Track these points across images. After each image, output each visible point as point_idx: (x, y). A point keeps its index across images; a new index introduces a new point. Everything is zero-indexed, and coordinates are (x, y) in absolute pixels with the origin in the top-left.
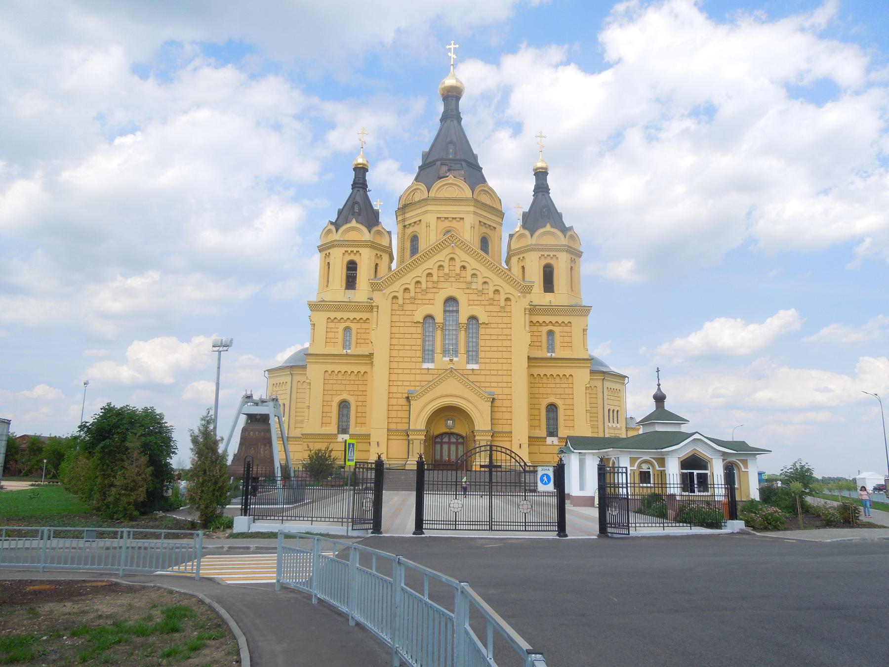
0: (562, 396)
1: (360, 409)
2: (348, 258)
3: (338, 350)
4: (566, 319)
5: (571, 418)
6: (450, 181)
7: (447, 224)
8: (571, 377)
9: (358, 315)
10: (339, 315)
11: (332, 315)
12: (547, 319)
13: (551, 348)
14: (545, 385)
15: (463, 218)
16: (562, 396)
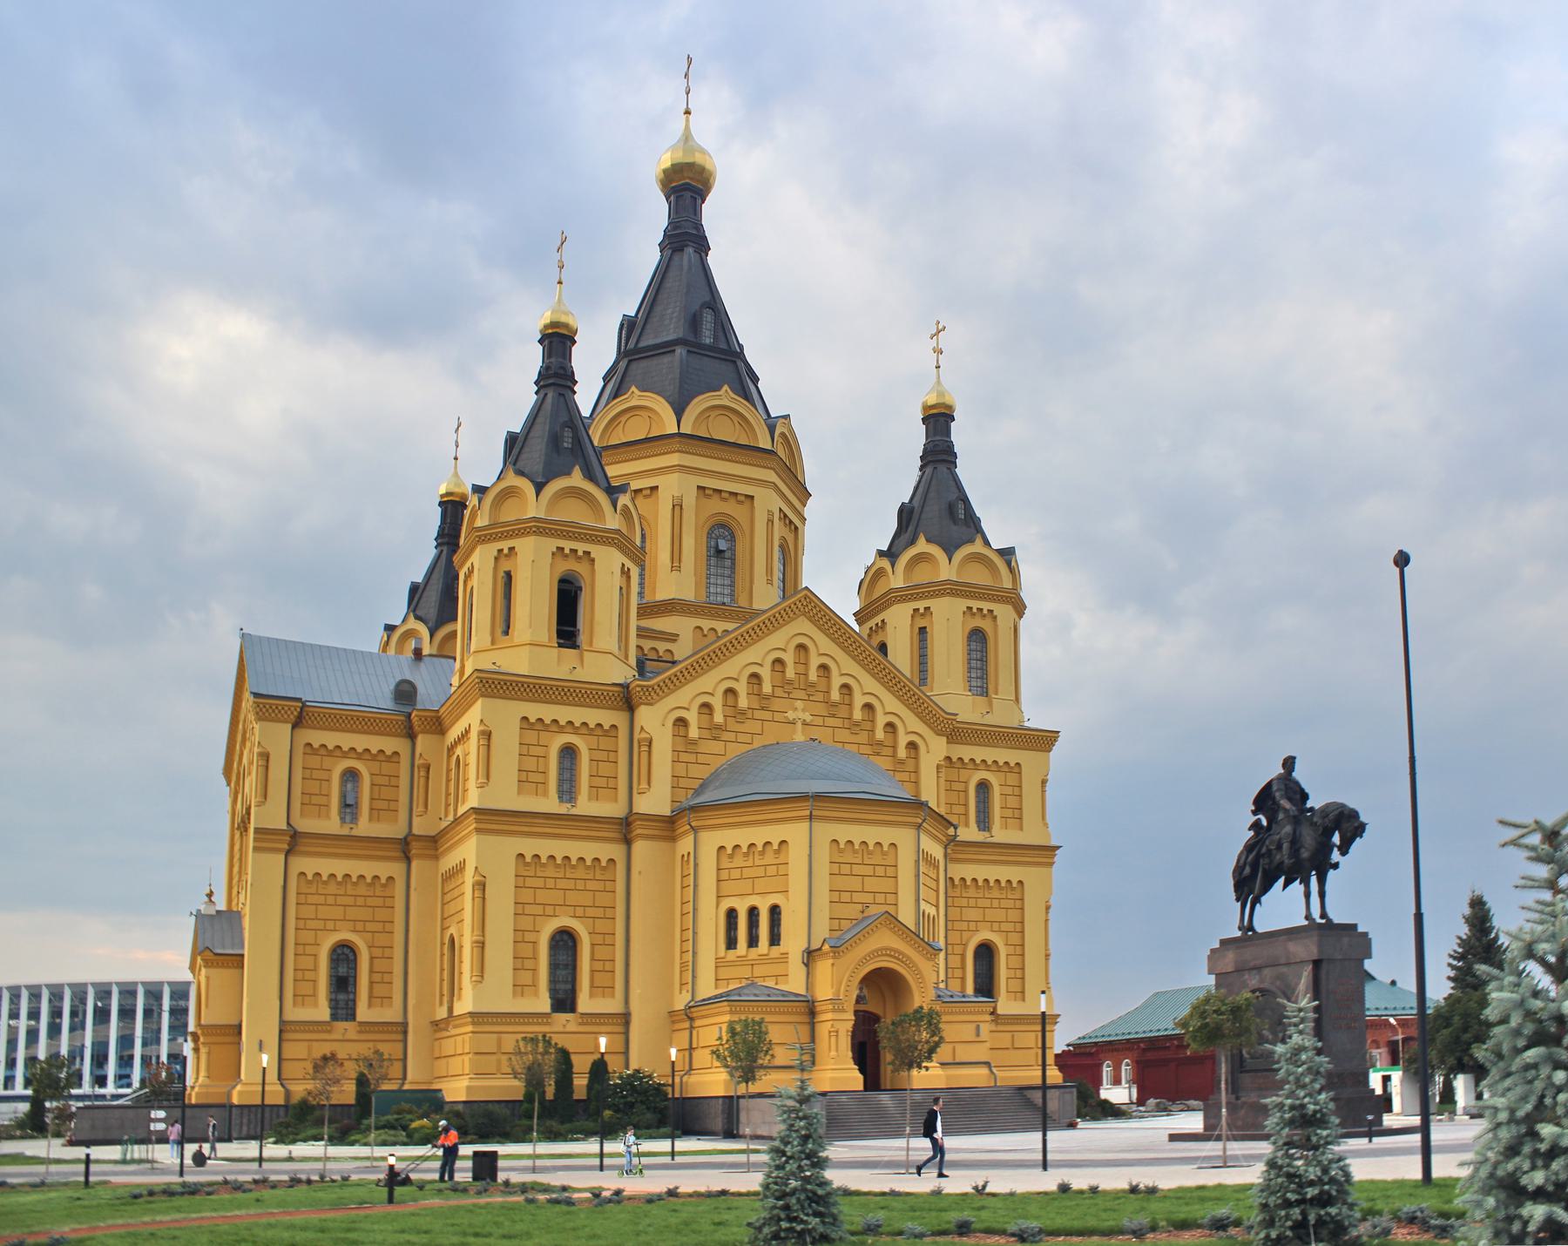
1: (602, 952)
2: (564, 566)
3: (550, 803)
9: (593, 716)
10: (548, 712)
11: (535, 711)
14: (972, 902)
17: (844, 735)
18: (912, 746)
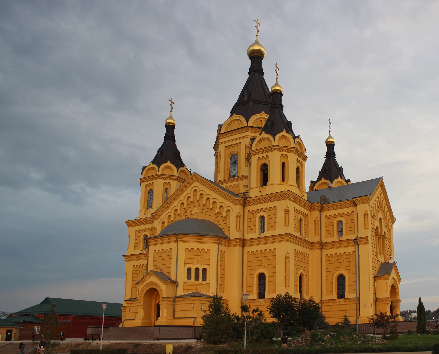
0: (269, 266)
2: (148, 188)
4: (272, 204)
5: (274, 283)
6: (235, 118)
7: (232, 149)
8: (275, 250)
12: (259, 207)
13: (262, 230)
15: (241, 143)
16: (269, 266)
17: (209, 213)
18: (228, 211)
